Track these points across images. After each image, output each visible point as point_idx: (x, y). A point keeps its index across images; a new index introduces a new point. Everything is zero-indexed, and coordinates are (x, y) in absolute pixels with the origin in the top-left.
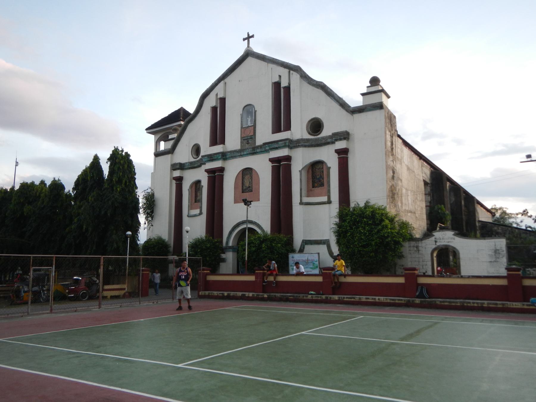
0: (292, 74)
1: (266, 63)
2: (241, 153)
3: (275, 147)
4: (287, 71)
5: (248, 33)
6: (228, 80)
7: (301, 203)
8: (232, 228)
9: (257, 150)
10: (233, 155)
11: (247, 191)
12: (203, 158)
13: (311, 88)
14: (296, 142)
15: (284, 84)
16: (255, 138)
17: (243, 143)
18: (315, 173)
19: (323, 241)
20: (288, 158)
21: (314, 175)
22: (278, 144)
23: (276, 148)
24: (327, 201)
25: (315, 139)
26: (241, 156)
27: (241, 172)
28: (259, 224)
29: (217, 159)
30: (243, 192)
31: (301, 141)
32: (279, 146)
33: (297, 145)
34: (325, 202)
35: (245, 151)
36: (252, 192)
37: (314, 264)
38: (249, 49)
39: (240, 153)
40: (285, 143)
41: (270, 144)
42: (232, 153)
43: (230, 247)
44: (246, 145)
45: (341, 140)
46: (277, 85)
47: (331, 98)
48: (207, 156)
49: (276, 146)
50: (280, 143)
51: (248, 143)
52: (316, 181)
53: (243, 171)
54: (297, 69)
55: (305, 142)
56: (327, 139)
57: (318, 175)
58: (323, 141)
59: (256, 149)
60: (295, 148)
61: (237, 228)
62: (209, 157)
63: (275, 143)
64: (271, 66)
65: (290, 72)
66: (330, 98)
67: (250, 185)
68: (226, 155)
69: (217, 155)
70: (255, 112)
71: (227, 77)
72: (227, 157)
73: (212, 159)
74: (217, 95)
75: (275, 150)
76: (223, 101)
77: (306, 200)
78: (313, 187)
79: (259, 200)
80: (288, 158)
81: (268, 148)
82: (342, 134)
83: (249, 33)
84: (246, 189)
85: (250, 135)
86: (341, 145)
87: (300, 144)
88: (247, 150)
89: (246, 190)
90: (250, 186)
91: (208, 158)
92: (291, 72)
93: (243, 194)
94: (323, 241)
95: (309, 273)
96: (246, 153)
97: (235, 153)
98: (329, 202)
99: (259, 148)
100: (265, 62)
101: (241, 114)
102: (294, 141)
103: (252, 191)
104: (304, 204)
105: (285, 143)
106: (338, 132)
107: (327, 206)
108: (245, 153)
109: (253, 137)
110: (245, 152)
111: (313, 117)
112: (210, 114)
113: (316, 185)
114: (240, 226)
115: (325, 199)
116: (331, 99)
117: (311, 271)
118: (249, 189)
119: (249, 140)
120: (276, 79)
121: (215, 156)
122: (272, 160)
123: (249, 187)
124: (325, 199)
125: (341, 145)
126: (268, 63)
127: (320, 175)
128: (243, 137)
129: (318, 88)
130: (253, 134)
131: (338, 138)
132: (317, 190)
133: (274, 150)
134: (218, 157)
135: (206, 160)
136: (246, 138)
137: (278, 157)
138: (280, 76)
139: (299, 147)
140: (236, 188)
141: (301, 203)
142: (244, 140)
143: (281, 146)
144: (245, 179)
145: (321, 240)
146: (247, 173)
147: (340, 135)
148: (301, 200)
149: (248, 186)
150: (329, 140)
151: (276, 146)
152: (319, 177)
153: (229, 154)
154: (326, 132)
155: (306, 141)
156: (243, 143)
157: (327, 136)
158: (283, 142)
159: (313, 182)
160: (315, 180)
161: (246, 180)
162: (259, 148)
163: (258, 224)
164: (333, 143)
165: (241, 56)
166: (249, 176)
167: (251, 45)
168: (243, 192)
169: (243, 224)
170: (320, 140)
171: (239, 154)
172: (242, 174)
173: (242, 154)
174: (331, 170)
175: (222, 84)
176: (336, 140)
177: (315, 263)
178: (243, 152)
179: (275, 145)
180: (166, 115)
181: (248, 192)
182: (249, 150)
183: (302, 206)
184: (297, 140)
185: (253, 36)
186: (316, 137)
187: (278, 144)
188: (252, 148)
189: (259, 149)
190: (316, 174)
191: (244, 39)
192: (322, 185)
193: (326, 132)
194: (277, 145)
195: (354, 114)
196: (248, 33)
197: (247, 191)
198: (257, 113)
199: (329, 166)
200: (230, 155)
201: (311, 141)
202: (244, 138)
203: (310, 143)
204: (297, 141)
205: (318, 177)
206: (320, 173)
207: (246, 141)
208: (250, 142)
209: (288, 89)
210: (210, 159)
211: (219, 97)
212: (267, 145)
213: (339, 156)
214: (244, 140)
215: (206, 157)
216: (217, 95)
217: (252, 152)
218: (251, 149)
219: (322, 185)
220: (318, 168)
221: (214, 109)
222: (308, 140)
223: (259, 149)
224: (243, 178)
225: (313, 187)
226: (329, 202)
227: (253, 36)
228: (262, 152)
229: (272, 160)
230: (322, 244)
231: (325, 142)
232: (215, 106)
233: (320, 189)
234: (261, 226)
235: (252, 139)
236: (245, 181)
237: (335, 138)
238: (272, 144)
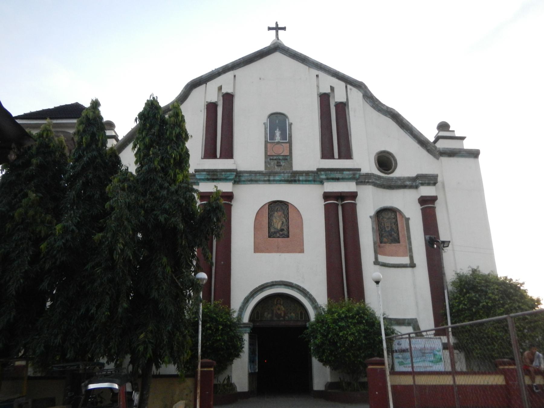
0: (351, 89)
1: (307, 67)
2: (269, 178)
3: (337, 177)
4: (343, 84)
5: (277, 23)
6: (238, 72)
7: (376, 262)
8: (251, 292)
9: (300, 177)
10: (253, 178)
11: (278, 235)
12: (197, 173)
13: (375, 114)
14: (364, 177)
15: (339, 96)
16: (291, 160)
17: (270, 164)
18: (383, 224)
19: (407, 321)
20: (353, 196)
21: (381, 227)
22: (342, 174)
23: (337, 179)
24: (409, 264)
25: (387, 178)
26: (269, 181)
27: (267, 206)
28: (306, 288)
29: (226, 180)
30: (269, 237)
31: (372, 177)
32: (344, 177)
33: (367, 181)
34: (406, 264)
35: (277, 175)
36: (288, 239)
37: (435, 355)
38: (278, 41)
39: (268, 177)
40: (354, 174)
41: (330, 172)
42: (253, 175)
43: (246, 326)
44: (276, 167)
45: (429, 184)
46: (324, 99)
47: (406, 131)
48: (207, 172)
49: (338, 175)
50: (345, 172)
51: (279, 165)
52: (384, 235)
53: (270, 205)
54: (359, 86)
55: (376, 179)
56: (405, 182)
57: (388, 227)
58: (399, 183)
59: (299, 176)
60: (360, 185)
61: (259, 293)
62: (211, 173)
63: (339, 172)
64: (315, 72)
65: (346, 87)
66: (404, 131)
67: (283, 228)
68: (240, 176)
69: (228, 173)
70: (291, 125)
71: (238, 68)
72: (243, 179)
73: (215, 177)
74: (220, 88)
75: (334, 181)
76: (228, 99)
77: (382, 259)
78: (381, 242)
79: (302, 251)
80: (353, 196)
81: (323, 177)
82: (432, 178)
83: (278, 23)
84: (275, 233)
85: (282, 154)
86: (427, 191)
87: (371, 181)
88: (282, 175)
89: (276, 234)
90: (285, 228)
91: (208, 175)
92: (349, 86)
93: (269, 238)
94: (407, 321)
95: (429, 369)
96: (278, 179)
97: (258, 175)
98: (412, 265)
99: (304, 174)
100: (306, 65)
101: (264, 124)
102: (362, 174)
103: (288, 237)
104: (380, 263)
105: (354, 174)
106: (427, 174)
107: (409, 270)
108: (277, 178)
109: (288, 158)
110: (277, 177)
111: (383, 149)
112: (203, 111)
113: (385, 240)
114: (265, 289)
115: (406, 260)
116: (406, 133)
117: (431, 367)
118: (281, 233)
119: (281, 161)
120: (328, 91)
121: (223, 173)
122: (327, 196)
123: (282, 230)
124: (406, 260)
125: (427, 191)
126: (309, 67)
127: (391, 227)
128: (270, 156)
129: (386, 115)
130: (288, 154)
131: (427, 182)
132: (389, 247)
133: (332, 181)
134: (228, 177)
135: (203, 177)
136: (275, 158)
137: (341, 193)
138: (332, 89)
139: (368, 184)
140: (257, 228)
141: (376, 262)
142: (273, 159)
143: (347, 177)
144: (274, 217)
145: (404, 320)
146: (277, 209)
147: (429, 178)
148: (376, 258)
149: (279, 228)
150: (408, 183)
151: (338, 175)
152: (389, 229)
153: (247, 175)
154: (399, 172)
155: (377, 178)
156: (270, 164)
157: (404, 177)
158: (351, 172)
159: (381, 236)
160: (383, 232)
161: (276, 218)
162: (304, 174)
163: (304, 289)
164: (416, 187)
165: (266, 48)
166: (280, 213)
167: (279, 38)
168: (269, 237)
169: (273, 287)
170: (394, 180)
171: (266, 179)
172: (269, 209)
173: (272, 178)
174: (411, 223)
175: (230, 74)
176: (422, 184)
177: (438, 353)
178: (274, 176)
179: (336, 175)
180: (51, 107)
181: (279, 237)
182: (286, 175)
183: (378, 267)
184: (366, 174)
185: (284, 29)
186: (386, 175)
187: (342, 174)
188: (292, 173)
189: (304, 177)
190: (384, 225)
191: (270, 29)
192: (397, 240)
193: (399, 172)
194: (340, 175)
195: (442, 156)
196: (277, 23)
197: (278, 235)
198: (293, 127)
199: (407, 216)
200: (249, 177)
201: (382, 179)
202: (272, 158)
203: (382, 181)
204: (365, 176)
205: (387, 229)
206: (390, 224)
207: (276, 162)
208: (282, 163)
209: (342, 107)
210: (212, 177)
211: (224, 91)
212: (323, 173)
213: (421, 206)
214: (273, 159)
215: (205, 173)
216: (220, 88)
217: (289, 179)
218: (289, 175)
219: (397, 240)
220: (387, 217)
221: (211, 108)
222: (379, 177)
223: (302, 176)
224: (270, 216)
225: (381, 242)
226: (412, 265)
227: (284, 29)
228: (307, 181)
229: (327, 196)
230: (405, 326)
231: (403, 184)
232: (216, 102)
233: (395, 246)
234: (308, 292)
235: (286, 161)
236: (274, 221)
237: (422, 181)
238: (332, 173)
